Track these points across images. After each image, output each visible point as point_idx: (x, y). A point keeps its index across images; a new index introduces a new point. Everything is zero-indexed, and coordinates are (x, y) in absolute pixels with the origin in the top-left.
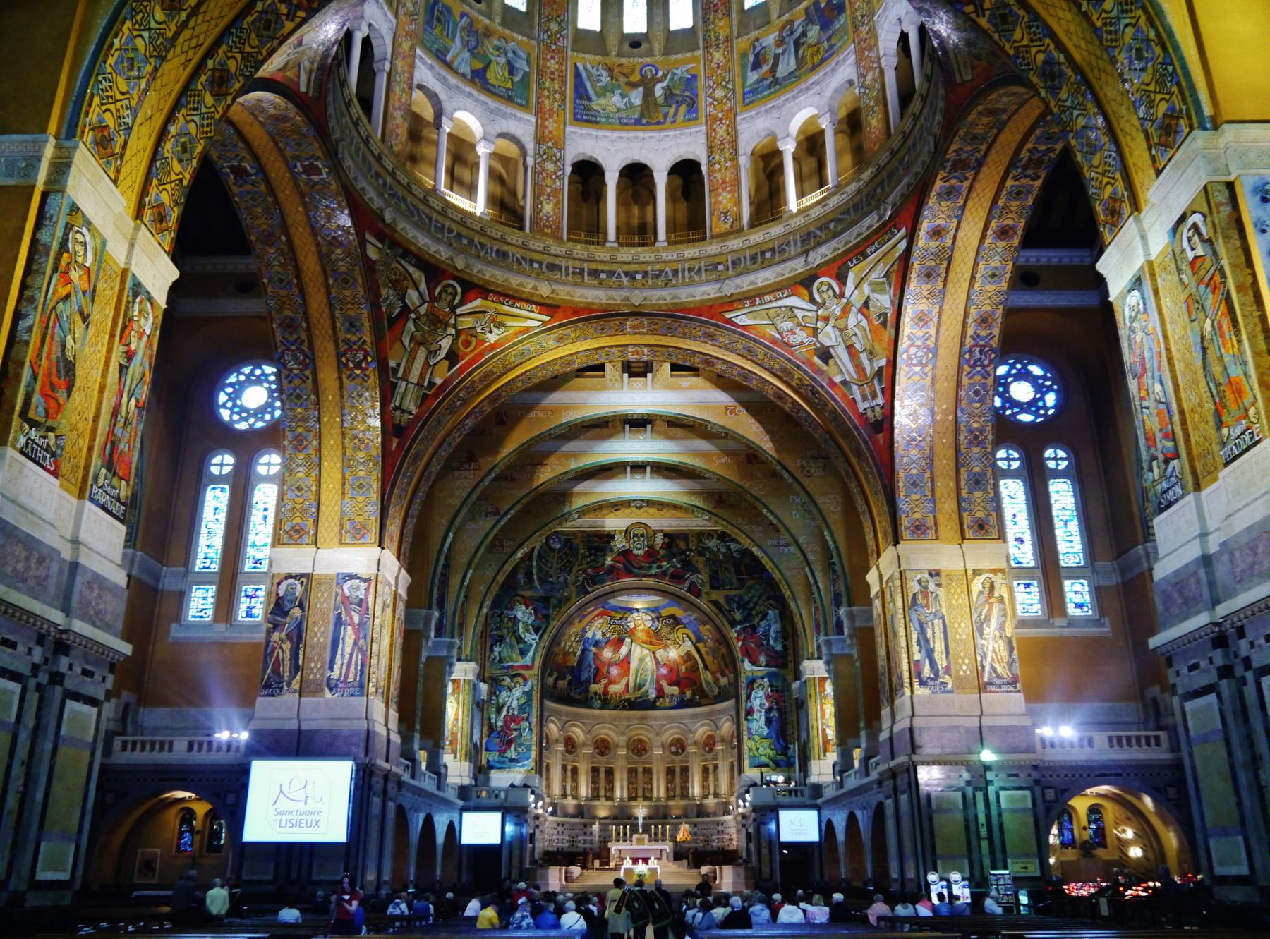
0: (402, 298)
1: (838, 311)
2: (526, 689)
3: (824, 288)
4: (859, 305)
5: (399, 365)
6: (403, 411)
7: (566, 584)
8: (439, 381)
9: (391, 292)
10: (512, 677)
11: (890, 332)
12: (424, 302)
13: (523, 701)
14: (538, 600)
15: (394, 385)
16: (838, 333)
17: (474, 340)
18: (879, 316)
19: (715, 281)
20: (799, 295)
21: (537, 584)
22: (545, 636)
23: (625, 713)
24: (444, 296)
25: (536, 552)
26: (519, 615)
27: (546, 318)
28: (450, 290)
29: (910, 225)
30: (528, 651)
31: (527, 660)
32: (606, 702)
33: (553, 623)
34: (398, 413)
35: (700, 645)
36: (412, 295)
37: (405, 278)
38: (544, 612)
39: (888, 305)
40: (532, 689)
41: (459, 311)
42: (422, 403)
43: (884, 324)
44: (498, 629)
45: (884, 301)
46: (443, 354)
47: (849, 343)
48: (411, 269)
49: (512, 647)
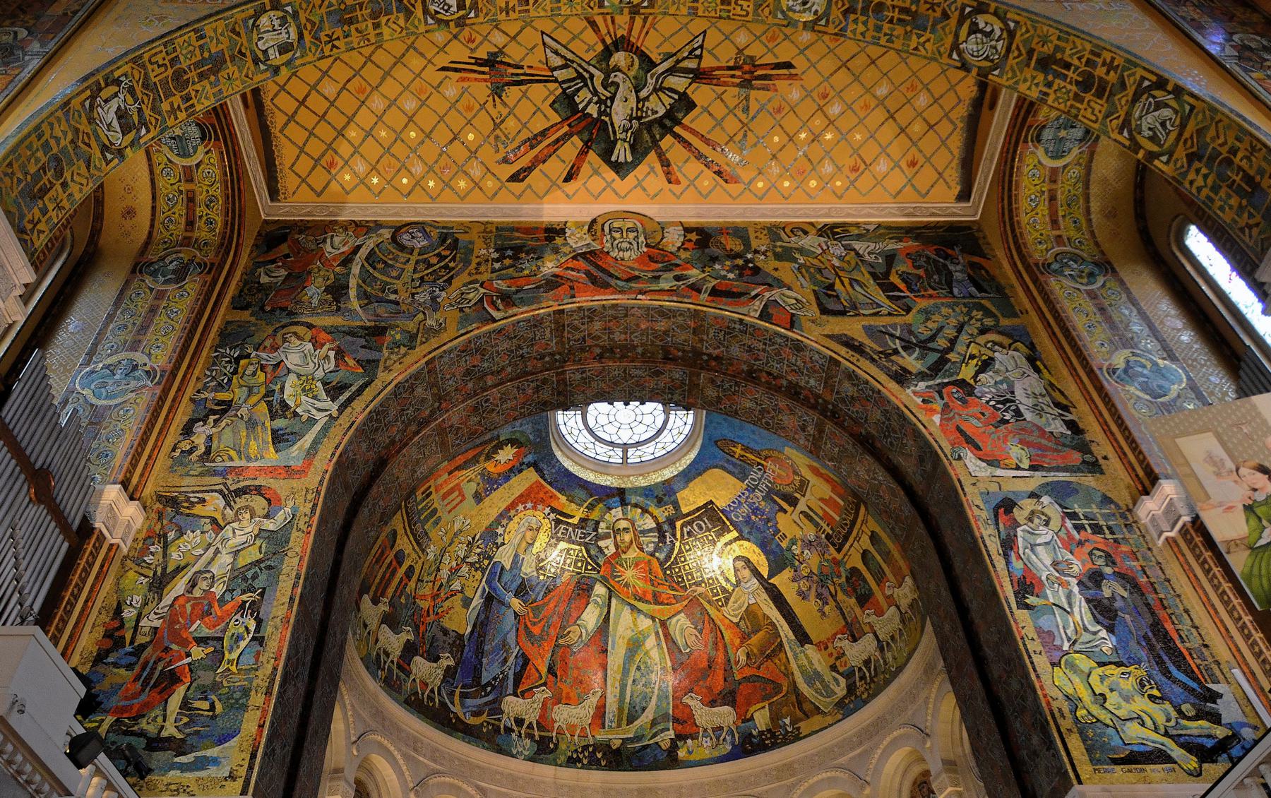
2: (270, 525)
7: (435, 304)
10: (231, 496)
13: (253, 555)
14: (351, 333)
21: (355, 304)
22: (358, 404)
23: (596, 778)
25: (363, 252)
26: (293, 360)
30: (299, 435)
31: (295, 453)
32: (544, 749)
33: (382, 376)
35: (782, 581)
38: (364, 354)
40: (289, 525)
44: (221, 387)
49: (252, 424)
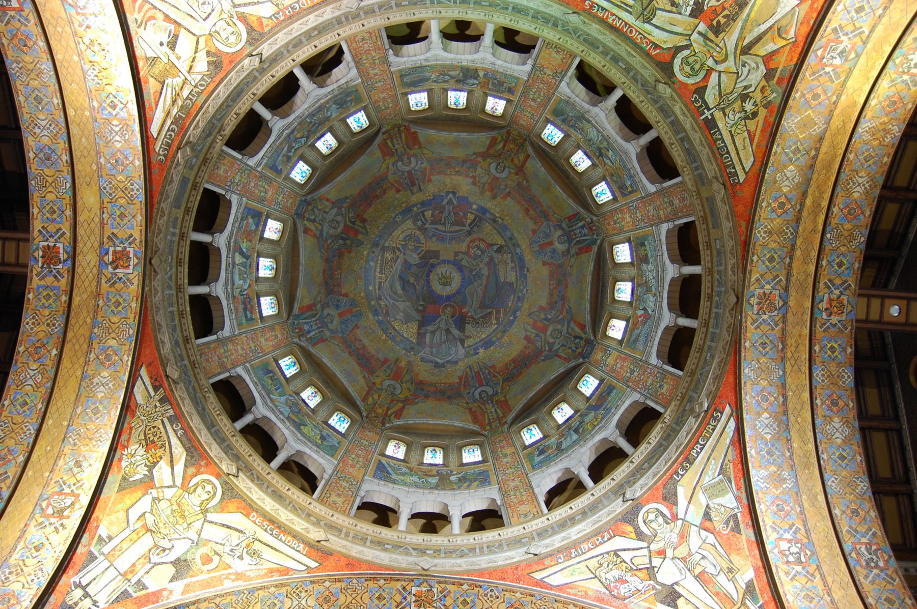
0: (151, 467)
1: (675, 538)
3: (652, 516)
4: (698, 520)
5: (110, 538)
6: (87, 595)
8: (152, 587)
9: (141, 451)
11: (748, 533)
12: (174, 486)
15: (92, 558)
16: (681, 565)
17: (216, 559)
18: (727, 523)
19: (520, 547)
20: (623, 535)
24: (199, 489)
27: (314, 564)
28: (209, 488)
29: (732, 397)
34: (79, 593)
36: (163, 469)
37: (163, 446)
39: (734, 504)
41: (210, 517)
42: (117, 600)
43: (737, 529)
45: (729, 501)
46: (172, 556)
47: (697, 571)
48: (175, 441)
